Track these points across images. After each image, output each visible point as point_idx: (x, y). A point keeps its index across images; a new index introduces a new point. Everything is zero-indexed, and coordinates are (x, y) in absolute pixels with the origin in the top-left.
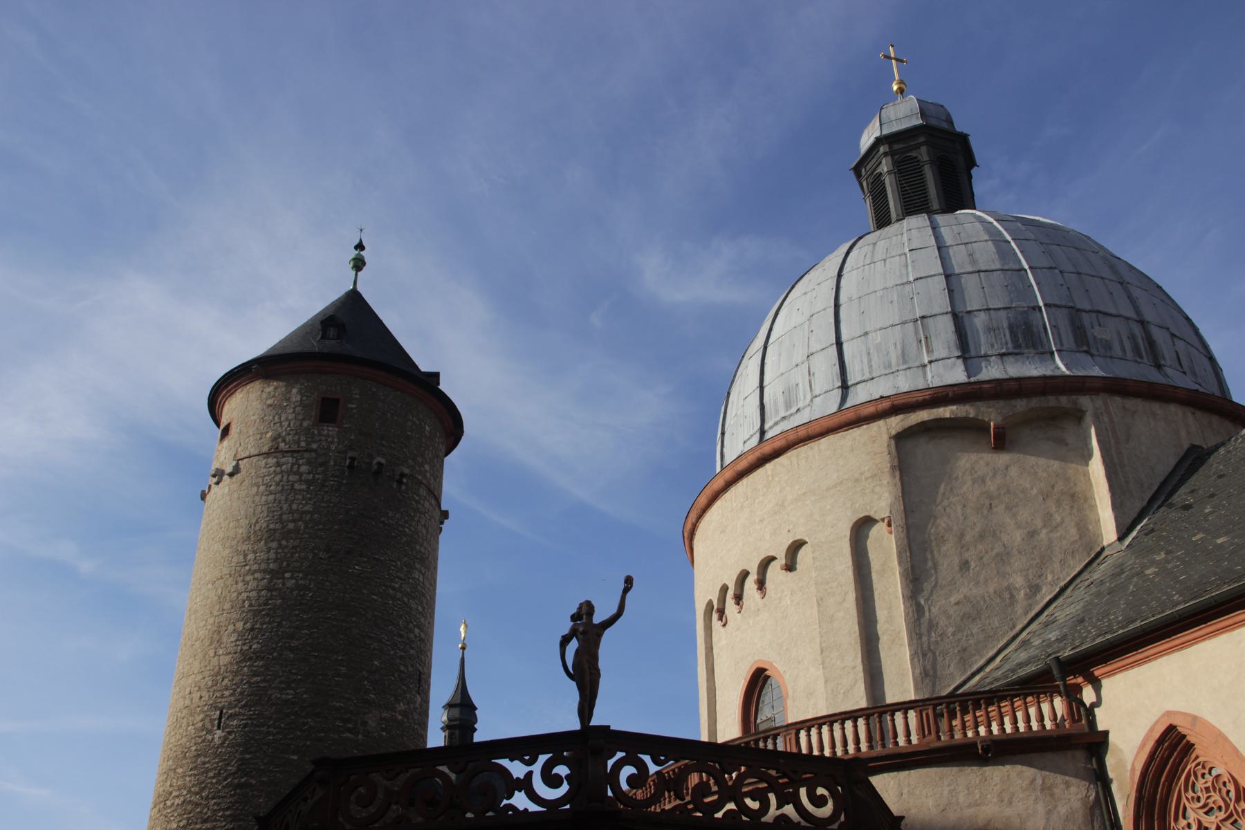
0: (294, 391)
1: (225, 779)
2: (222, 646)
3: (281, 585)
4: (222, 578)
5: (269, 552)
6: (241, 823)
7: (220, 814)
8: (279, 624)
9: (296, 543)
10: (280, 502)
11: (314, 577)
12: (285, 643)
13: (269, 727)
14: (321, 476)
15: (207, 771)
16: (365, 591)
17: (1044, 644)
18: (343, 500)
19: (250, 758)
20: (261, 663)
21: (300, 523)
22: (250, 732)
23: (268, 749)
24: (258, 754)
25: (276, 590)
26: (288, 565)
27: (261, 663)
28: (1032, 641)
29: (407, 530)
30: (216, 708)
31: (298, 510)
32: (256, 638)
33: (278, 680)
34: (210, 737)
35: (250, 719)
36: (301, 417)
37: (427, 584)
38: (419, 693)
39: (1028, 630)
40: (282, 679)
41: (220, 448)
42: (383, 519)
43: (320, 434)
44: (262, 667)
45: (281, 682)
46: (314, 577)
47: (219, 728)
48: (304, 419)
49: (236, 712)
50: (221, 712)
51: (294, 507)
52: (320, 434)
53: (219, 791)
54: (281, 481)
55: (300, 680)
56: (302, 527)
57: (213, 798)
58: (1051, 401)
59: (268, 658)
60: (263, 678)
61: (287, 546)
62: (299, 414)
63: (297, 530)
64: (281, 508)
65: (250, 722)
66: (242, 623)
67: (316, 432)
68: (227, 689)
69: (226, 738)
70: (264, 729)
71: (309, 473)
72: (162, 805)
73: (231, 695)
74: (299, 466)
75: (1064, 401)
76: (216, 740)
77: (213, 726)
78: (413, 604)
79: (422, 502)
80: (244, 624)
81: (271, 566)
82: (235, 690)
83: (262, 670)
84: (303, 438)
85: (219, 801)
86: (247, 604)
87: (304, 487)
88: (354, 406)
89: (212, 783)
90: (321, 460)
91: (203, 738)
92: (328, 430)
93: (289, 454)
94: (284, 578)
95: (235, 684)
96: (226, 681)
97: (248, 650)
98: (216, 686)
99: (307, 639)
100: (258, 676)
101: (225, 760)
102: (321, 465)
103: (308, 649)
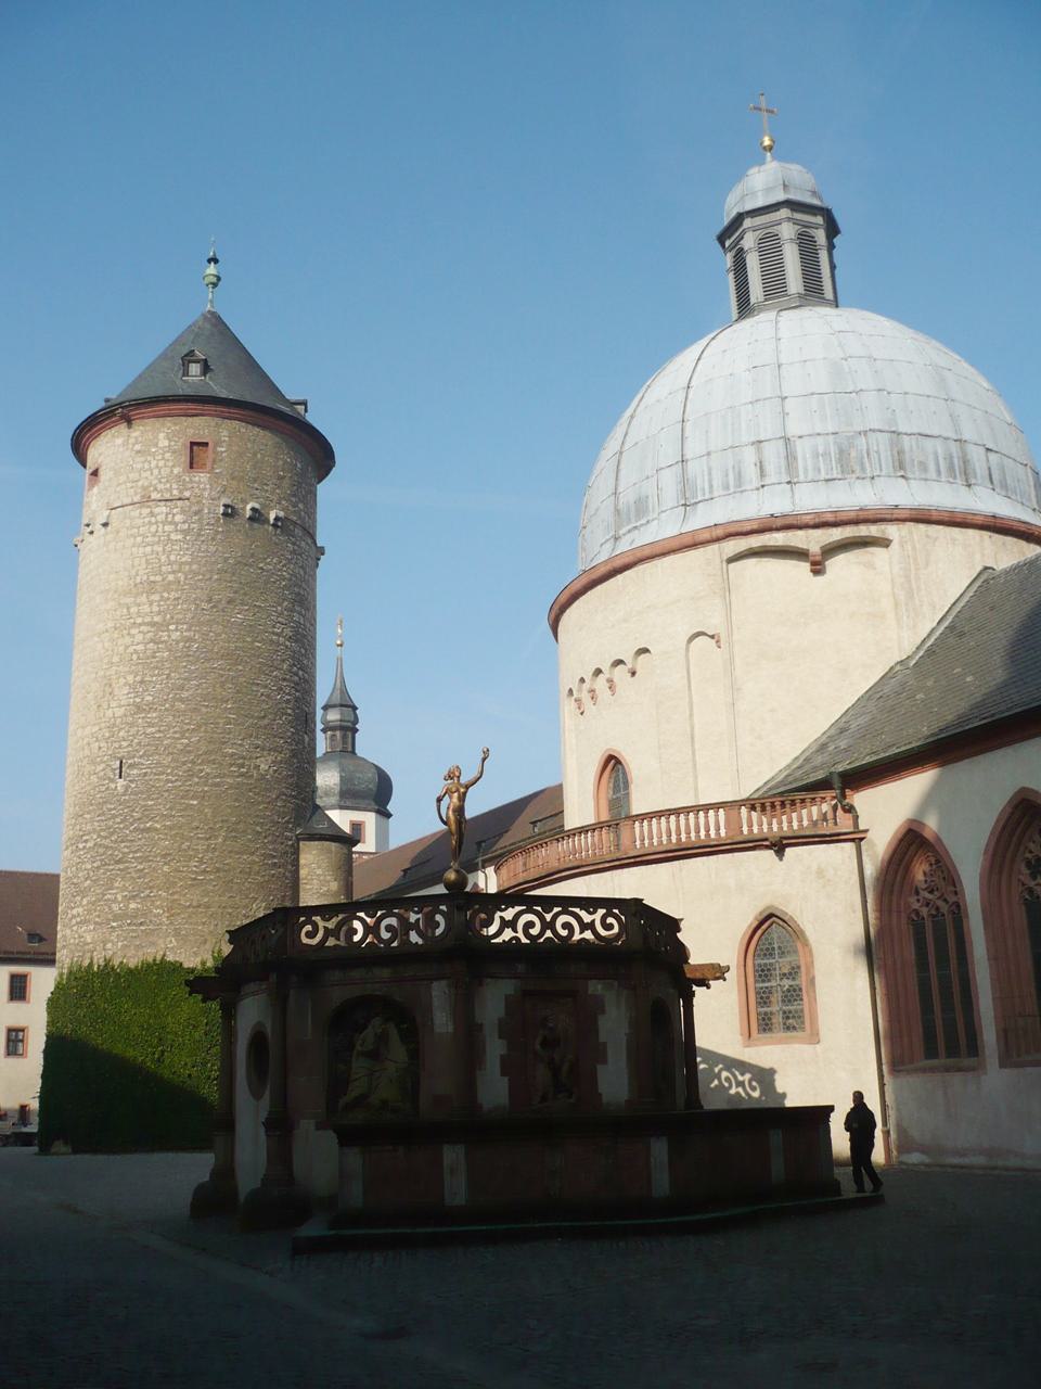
0: (161, 435)
4: (107, 631)
5: (151, 605)
7: (131, 856)
8: (168, 676)
13: (168, 775)
15: (114, 816)
18: (220, 548)
20: (154, 715)
26: (172, 618)
27: (154, 715)
33: (172, 731)
34: (113, 786)
36: (170, 464)
45: (175, 732)
47: (120, 777)
50: (121, 762)
51: (172, 558)
52: (191, 481)
56: (182, 579)
57: (122, 842)
61: (168, 599)
64: (160, 560)
65: (149, 770)
67: (187, 479)
70: (163, 777)
71: (184, 522)
74: (174, 515)
81: (156, 619)
84: (174, 486)
86: (135, 657)
87: (180, 537)
88: (223, 449)
89: (120, 829)
90: (195, 508)
93: (163, 503)
94: (168, 630)
96: (121, 734)
102: (196, 513)
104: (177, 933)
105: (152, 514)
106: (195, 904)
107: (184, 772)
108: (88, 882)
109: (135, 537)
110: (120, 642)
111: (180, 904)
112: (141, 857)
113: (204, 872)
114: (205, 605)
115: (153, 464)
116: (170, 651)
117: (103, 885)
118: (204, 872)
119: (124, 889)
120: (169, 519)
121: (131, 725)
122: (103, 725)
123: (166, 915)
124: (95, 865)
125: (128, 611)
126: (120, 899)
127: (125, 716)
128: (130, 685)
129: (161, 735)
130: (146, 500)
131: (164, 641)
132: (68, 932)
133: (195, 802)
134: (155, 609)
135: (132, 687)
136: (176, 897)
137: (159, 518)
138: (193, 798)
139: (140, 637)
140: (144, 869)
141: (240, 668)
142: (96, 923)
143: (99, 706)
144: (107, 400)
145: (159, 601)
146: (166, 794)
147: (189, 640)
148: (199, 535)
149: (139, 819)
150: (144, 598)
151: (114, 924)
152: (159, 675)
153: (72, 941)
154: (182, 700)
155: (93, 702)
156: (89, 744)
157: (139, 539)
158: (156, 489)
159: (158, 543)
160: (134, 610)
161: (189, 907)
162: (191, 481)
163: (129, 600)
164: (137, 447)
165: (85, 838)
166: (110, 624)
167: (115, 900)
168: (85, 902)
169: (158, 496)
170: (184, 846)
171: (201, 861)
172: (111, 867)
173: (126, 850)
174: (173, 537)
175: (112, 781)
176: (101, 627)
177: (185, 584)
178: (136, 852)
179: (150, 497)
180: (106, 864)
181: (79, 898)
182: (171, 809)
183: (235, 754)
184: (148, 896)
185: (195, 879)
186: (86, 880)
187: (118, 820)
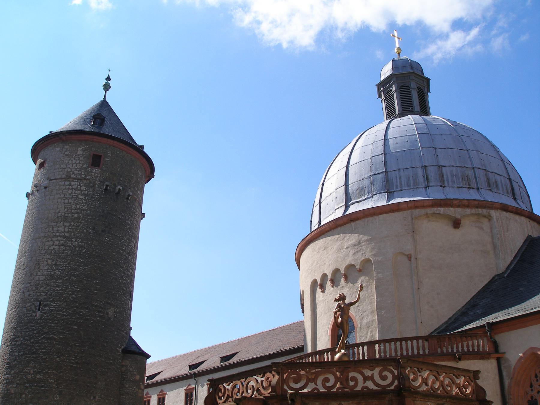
2: (40, 271)
3: (70, 244)
7: (40, 351)
9: (78, 224)
12: (72, 272)
13: (64, 312)
14: (91, 193)
15: (33, 330)
16: (110, 251)
21: (80, 215)
22: (55, 314)
23: (63, 322)
24: (58, 325)
25: (68, 246)
26: (74, 235)
30: (37, 301)
31: (79, 208)
32: (58, 269)
34: (35, 314)
35: (55, 308)
36: (82, 162)
40: (70, 290)
44: (60, 283)
45: (70, 291)
48: (84, 164)
49: (48, 303)
51: (78, 206)
53: (40, 340)
55: (79, 291)
57: (37, 343)
58: (480, 211)
59: (63, 279)
61: (74, 226)
62: (81, 161)
63: (79, 218)
64: (71, 207)
65: (54, 309)
68: (43, 292)
69: (42, 316)
70: (61, 313)
71: (86, 191)
73: (46, 295)
74: (81, 187)
75: (485, 211)
76: (38, 316)
77: (36, 309)
81: (66, 235)
82: (47, 293)
83: (61, 284)
84: (83, 173)
86: (53, 252)
91: (31, 314)
92: (96, 170)
94: (72, 241)
96: (42, 289)
97: (54, 274)
98: (37, 290)
99: (82, 272)
101: (42, 326)
102: (92, 187)
105: (70, 185)
107: (72, 312)
110: (47, 244)
112: (45, 352)
114: (91, 231)
115: (74, 161)
116: (71, 251)
117: (23, 364)
120: (79, 188)
124: (20, 354)
125: (53, 229)
127: (45, 280)
128: (49, 265)
129: (62, 292)
130: (68, 178)
131: (69, 246)
133: (76, 327)
134: (66, 229)
136: (61, 374)
137: (74, 187)
139: (57, 242)
140: (46, 358)
142: (17, 384)
143: (31, 274)
145: (69, 226)
147: (82, 247)
148: (92, 197)
150: (61, 224)
151: (28, 385)
152: (64, 262)
158: (73, 173)
160: (55, 229)
162: (91, 172)
163: (54, 224)
164: (67, 153)
165: (15, 339)
166: (42, 235)
167: (29, 373)
168: (12, 372)
170: (68, 349)
172: (29, 356)
173: (38, 348)
175: (34, 312)
177: (83, 220)
178: (43, 349)
180: (26, 354)
184: (47, 372)
186: (14, 361)
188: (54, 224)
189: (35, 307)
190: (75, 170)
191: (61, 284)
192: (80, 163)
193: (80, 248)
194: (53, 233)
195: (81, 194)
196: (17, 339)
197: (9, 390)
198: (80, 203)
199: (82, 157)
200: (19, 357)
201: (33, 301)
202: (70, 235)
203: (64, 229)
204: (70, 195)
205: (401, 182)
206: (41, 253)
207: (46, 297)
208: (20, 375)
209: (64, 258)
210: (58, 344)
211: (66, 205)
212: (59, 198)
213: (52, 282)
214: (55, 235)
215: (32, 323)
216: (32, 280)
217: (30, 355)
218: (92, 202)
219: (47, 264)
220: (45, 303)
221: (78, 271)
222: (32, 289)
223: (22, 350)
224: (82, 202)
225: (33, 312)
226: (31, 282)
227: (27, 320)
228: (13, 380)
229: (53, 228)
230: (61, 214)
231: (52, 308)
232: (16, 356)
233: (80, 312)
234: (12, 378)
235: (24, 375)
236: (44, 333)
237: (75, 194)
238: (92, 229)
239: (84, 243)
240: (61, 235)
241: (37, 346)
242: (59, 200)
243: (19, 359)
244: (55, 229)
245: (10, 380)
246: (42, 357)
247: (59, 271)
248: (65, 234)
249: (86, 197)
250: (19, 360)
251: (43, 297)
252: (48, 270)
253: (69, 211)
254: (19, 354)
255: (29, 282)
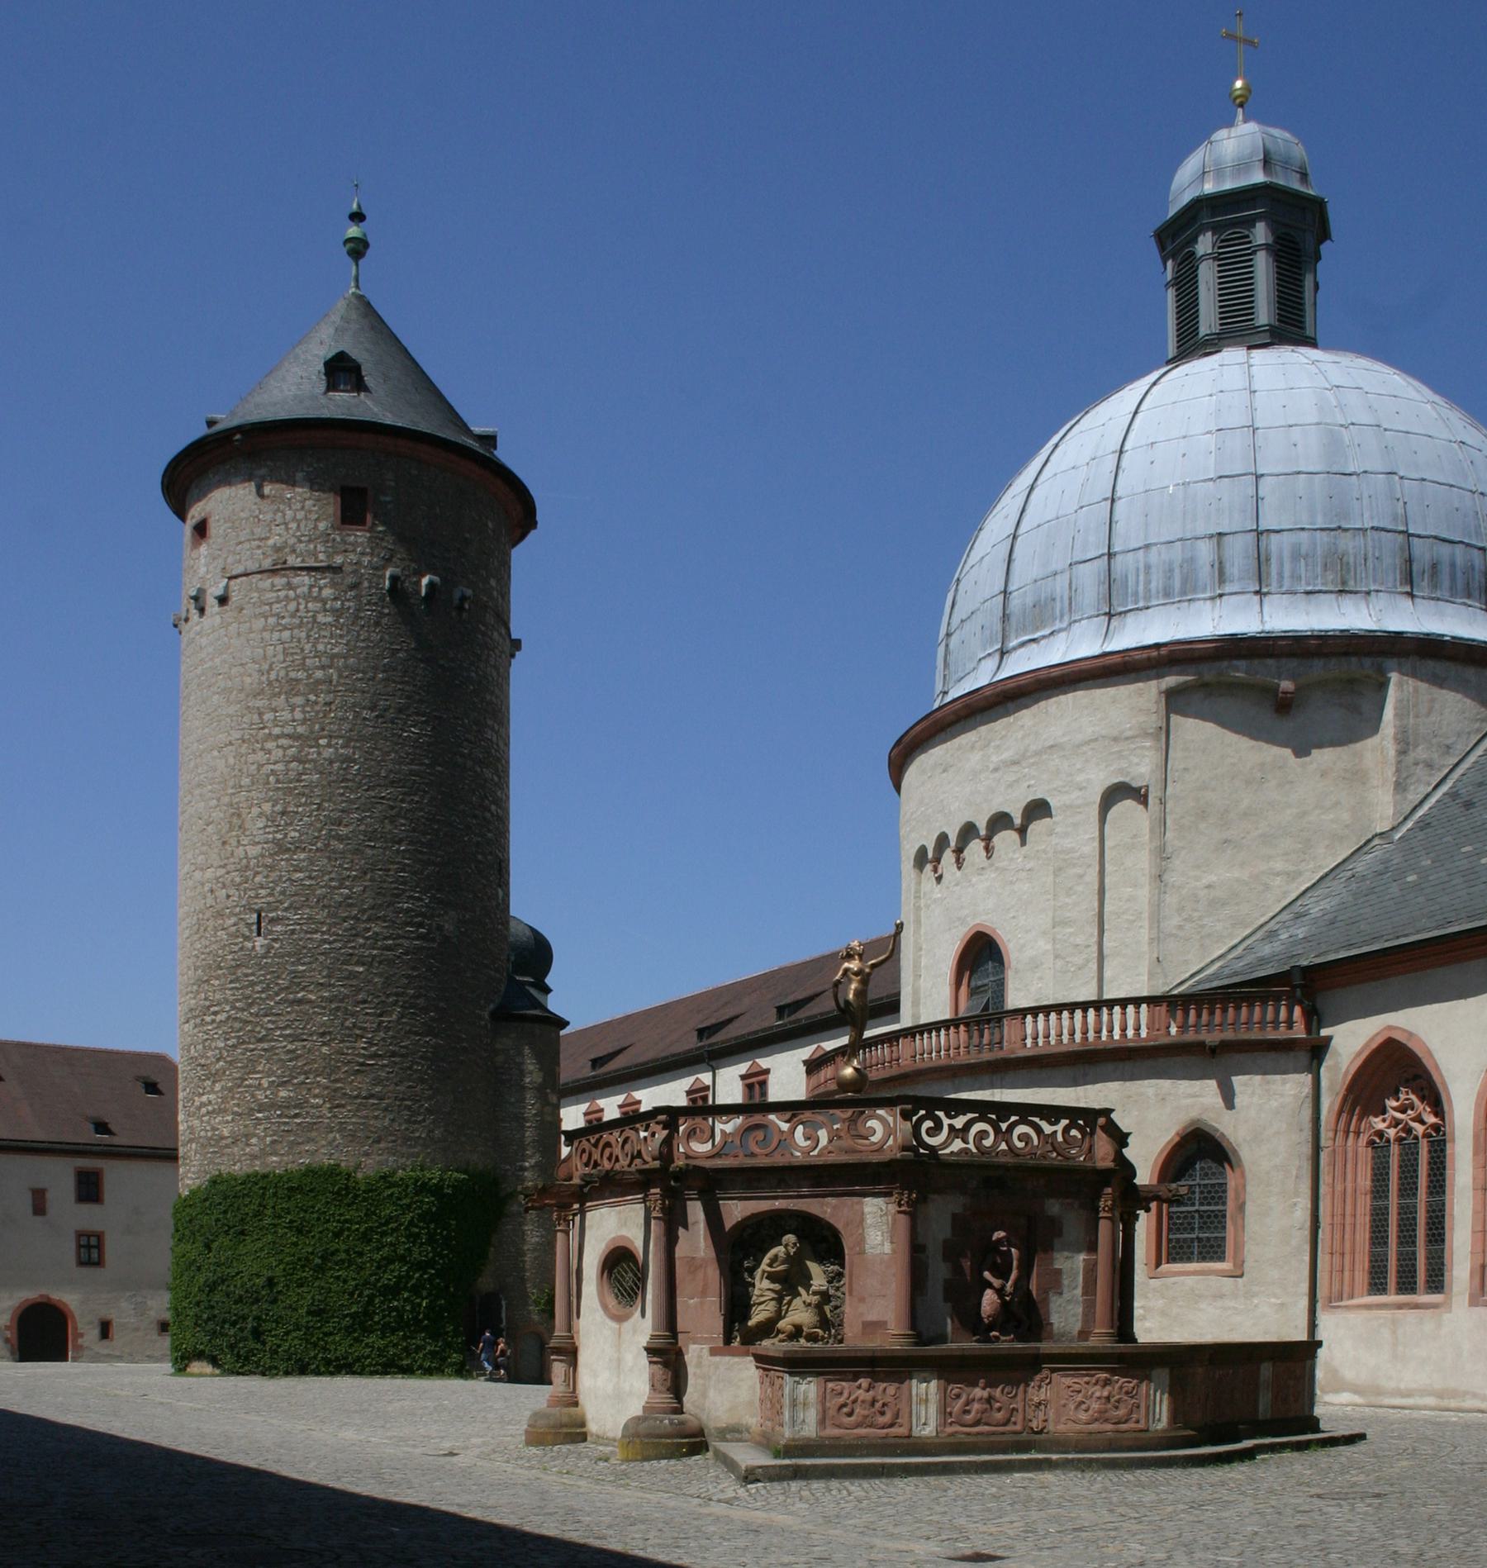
1: (277, 994)
2: (247, 833)
3: (315, 756)
4: (231, 744)
5: (293, 711)
6: (306, 1043)
7: (278, 1033)
10: (299, 641)
11: (358, 745)
12: (331, 830)
13: (323, 933)
14: (352, 604)
15: (253, 984)
17: (1291, 940)
18: (387, 637)
19: (304, 971)
20: (302, 856)
21: (331, 671)
22: (300, 940)
23: (326, 960)
24: (314, 966)
28: (1280, 932)
29: (473, 674)
30: (252, 910)
31: (325, 652)
32: (291, 824)
33: (326, 878)
34: (249, 945)
35: (299, 924)
37: (501, 744)
38: (500, 886)
39: (1277, 919)
41: (194, 554)
42: (441, 662)
43: (344, 542)
44: (304, 860)
45: (331, 880)
46: (358, 745)
47: (259, 934)
49: (278, 915)
50: (259, 916)
51: (321, 647)
53: (272, 1008)
54: (297, 610)
55: (356, 876)
60: (307, 874)
61: (316, 703)
64: (302, 650)
65: (298, 927)
66: (270, 804)
67: (338, 539)
68: (262, 888)
69: (269, 948)
70: (317, 936)
72: (198, 1021)
74: (321, 589)
76: (258, 948)
77: (251, 931)
78: (488, 773)
79: (490, 633)
80: (273, 806)
81: (300, 729)
82: (273, 889)
83: (305, 864)
84: (320, 548)
85: (274, 1019)
88: (388, 499)
89: (260, 998)
91: (240, 945)
92: (356, 536)
94: (318, 746)
95: (272, 882)
96: (258, 879)
98: (246, 883)
99: (359, 825)
100: (301, 871)
103: (362, 837)
104: (342, 1128)
105: (289, 586)
106: (364, 1094)
107: (345, 931)
108: (221, 1063)
109: (266, 618)
110: (251, 758)
111: (345, 1094)
112: (288, 1035)
113: (374, 1056)
114: (366, 714)
115: (289, 513)
116: (321, 773)
117: (241, 1067)
118: (374, 1056)
119: (270, 1073)
120: (315, 594)
121: (272, 868)
122: (232, 867)
123: (328, 1105)
124: (230, 1043)
125: (261, 718)
126: (266, 1085)
127: (263, 856)
128: (266, 817)
129: (313, 882)
130: (278, 569)
131: (312, 760)
132: (197, 1123)
133: (361, 969)
134: (298, 715)
135: (271, 819)
138: (359, 963)
140: (296, 1049)
141: (416, 799)
143: (224, 843)
144: (211, 423)
145: (303, 706)
146: (321, 958)
147: (349, 760)
148: (357, 618)
149: (287, 988)
152: (305, 804)
153: (202, 1134)
154: (340, 838)
155: (215, 837)
156: (212, 891)
157: (272, 620)
158: (294, 551)
159: (300, 626)
160: (268, 716)
161: (356, 1097)
162: (344, 542)
163: (259, 703)
166: (236, 735)
169: (298, 563)
170: (347, 1024)
171: (370, 1043)
172: (252, 1046)
173: (270, 1026)
174: (321, 618)
175: (247, 938)
176: (223, 737)
179: (285, 563)
180: (244, 1042)
181: (208, 1083)
182: (329, 976)
183: (412, 910)
185: (362, 1064)
186: (218, 1060)
187: (258, 988)
188: (259, 703)
189: (249, 925)
190: (296, 540)
191: (305, 864)
192: (306, 518)
193: (343, 762)
194: (262, 728)
195: (325, 610)
196: (216, 1009)
197: (218, 1129)
198: (325, 637)
199: (310, 499)
200: (228, 1051)
201: (240, 912)
202: (312, 732)
203: (293, 716)
204: (293, 616)
205: (1148, 582)
206: (241, 787)
207: (271, 899)
208: (239, 1093)
209: (303, 795)
210: (320, 1014)
211: (286, 645)
212: (264, 629)
213: (282, 860)
214: (270, 734)
215: (247, 967)
216: (228, 858)
217: (253, 1044)
218: (358, 632)
219: (261, 815)
220: (270, 915)
221: (346, 826)
222: (232, 881)
223: (233, 1035)
224: (331, 634)
225: (245, 940)
226: (226, 865)
227: (233, 960)
228: (223, 1106)
229: (261, 714)
230: (278, 675)
231: (291, 927)
232: (220, 1049)
233: (369, 930)
234: (220, 1100)
235: (246, 1091)
236: (281, 990)
237: (308, 612)
238: (369, 709)
239: (354, 747)
240: (286, 731)
241: (269, 1021)
242: (264, 634)
243: (228, 1056)
244: (268, 716)
245: (216, 1107)
246: (285, 1047)
247: (295, 830)
248: (295, 729)
249: (339, 617)
250: (229, 1059)
251: (263, 900)
252: (267, 830)
253: (297, 662)
254: (226, 1045)
255: (222, 864)
